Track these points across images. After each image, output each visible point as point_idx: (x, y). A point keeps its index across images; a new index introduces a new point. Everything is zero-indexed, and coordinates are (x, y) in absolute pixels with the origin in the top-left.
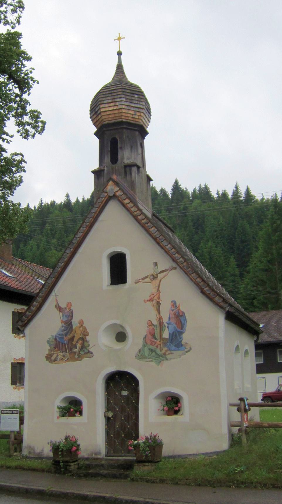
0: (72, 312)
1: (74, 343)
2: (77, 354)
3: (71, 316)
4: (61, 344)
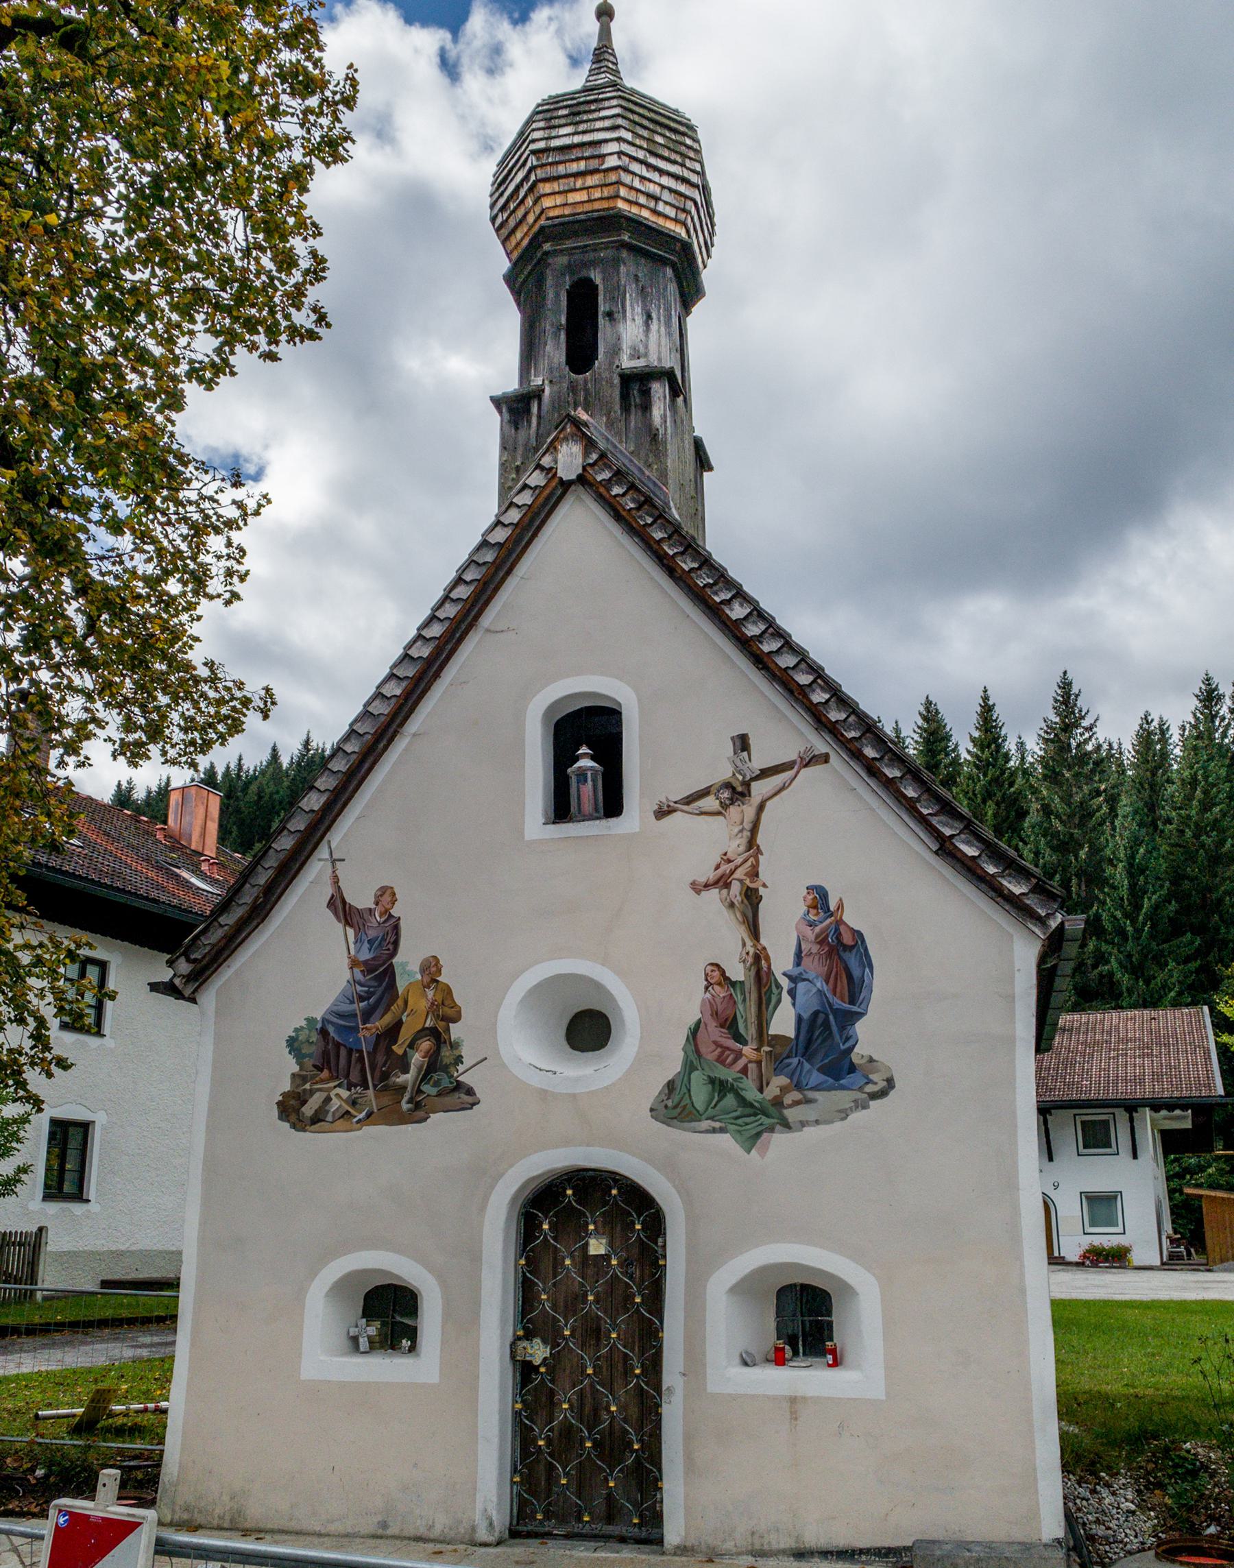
0: (396, 928)
1: (398, 1049)
2: (407, 1097)
3: (392, 936)
4: (343, 1052)
